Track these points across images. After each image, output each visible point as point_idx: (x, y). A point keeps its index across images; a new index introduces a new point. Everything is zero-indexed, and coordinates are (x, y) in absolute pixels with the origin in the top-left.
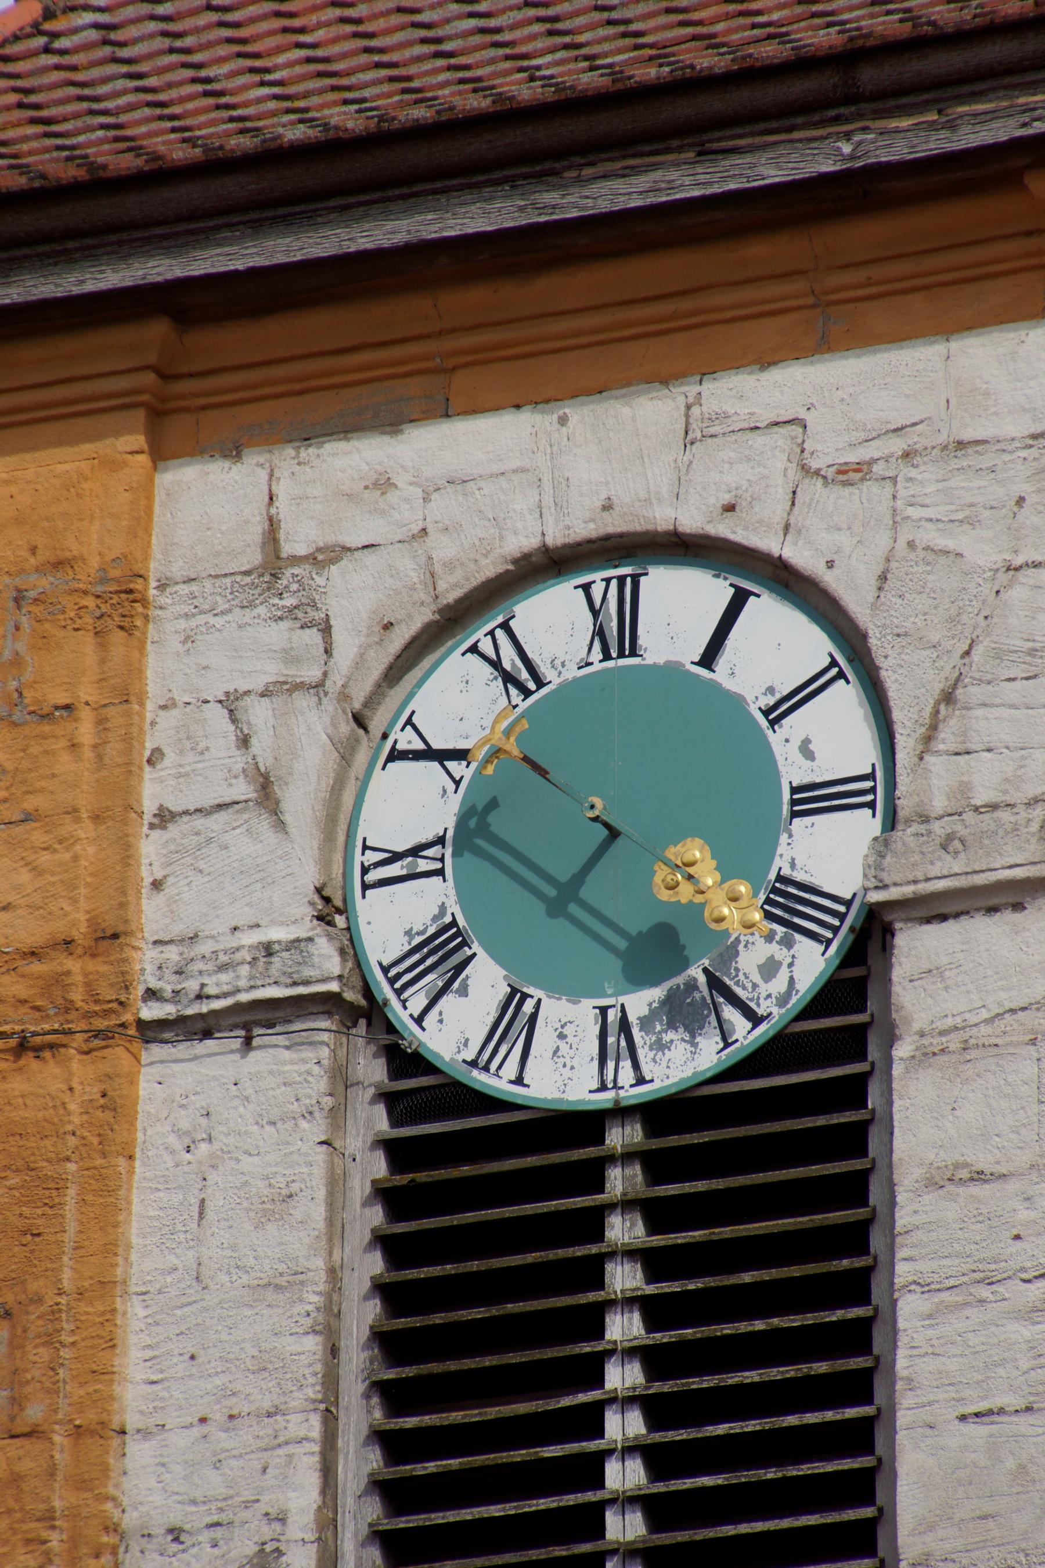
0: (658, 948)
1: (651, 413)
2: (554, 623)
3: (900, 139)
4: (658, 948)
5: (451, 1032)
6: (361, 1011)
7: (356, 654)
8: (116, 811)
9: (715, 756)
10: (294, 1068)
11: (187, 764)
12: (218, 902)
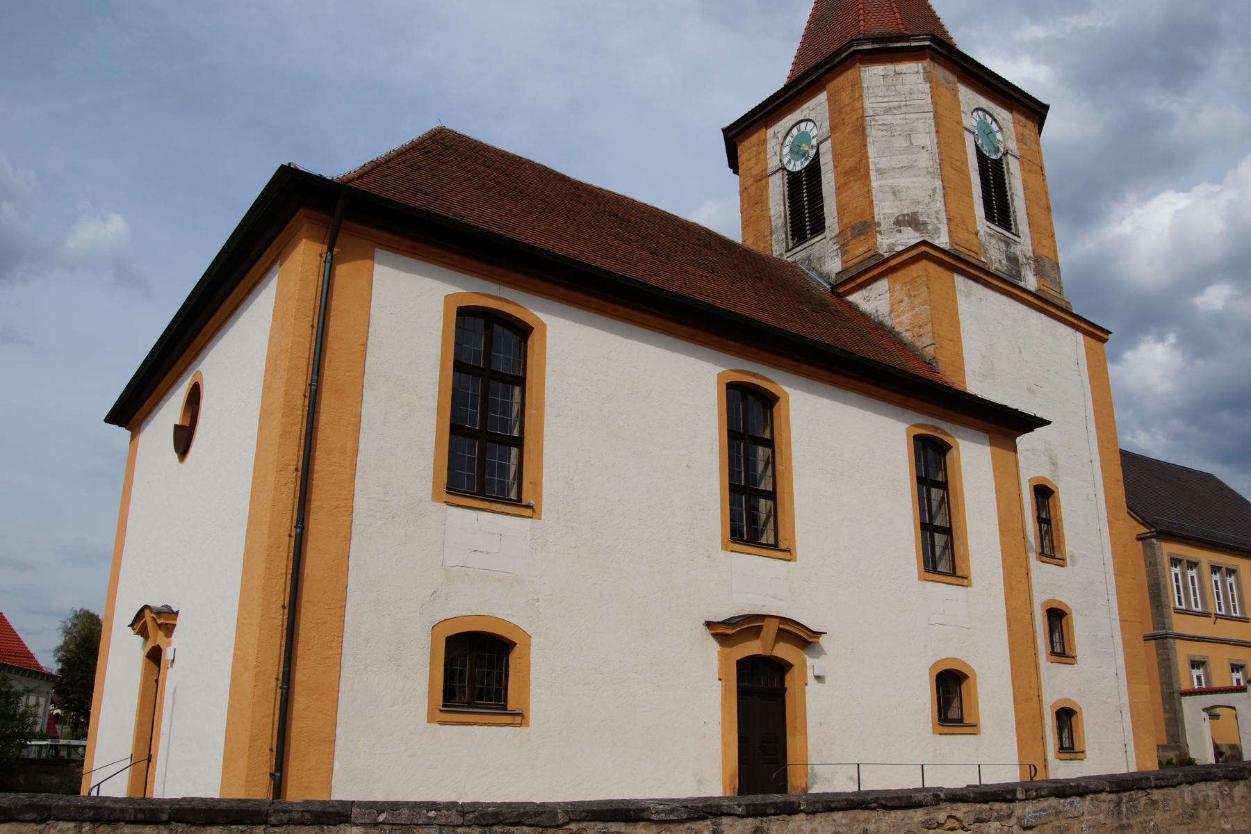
0: (804, 155)
1: (799, 111)
2: (795, 131)
3: (809, 80)
4: (804, 155)
5: (790, 168)
6: (784, 169)
7: (781, 140)
8: (766, 159)
9: (805, 136)
10: (779, 175)
11: (770, 153)
12: (773, 163)
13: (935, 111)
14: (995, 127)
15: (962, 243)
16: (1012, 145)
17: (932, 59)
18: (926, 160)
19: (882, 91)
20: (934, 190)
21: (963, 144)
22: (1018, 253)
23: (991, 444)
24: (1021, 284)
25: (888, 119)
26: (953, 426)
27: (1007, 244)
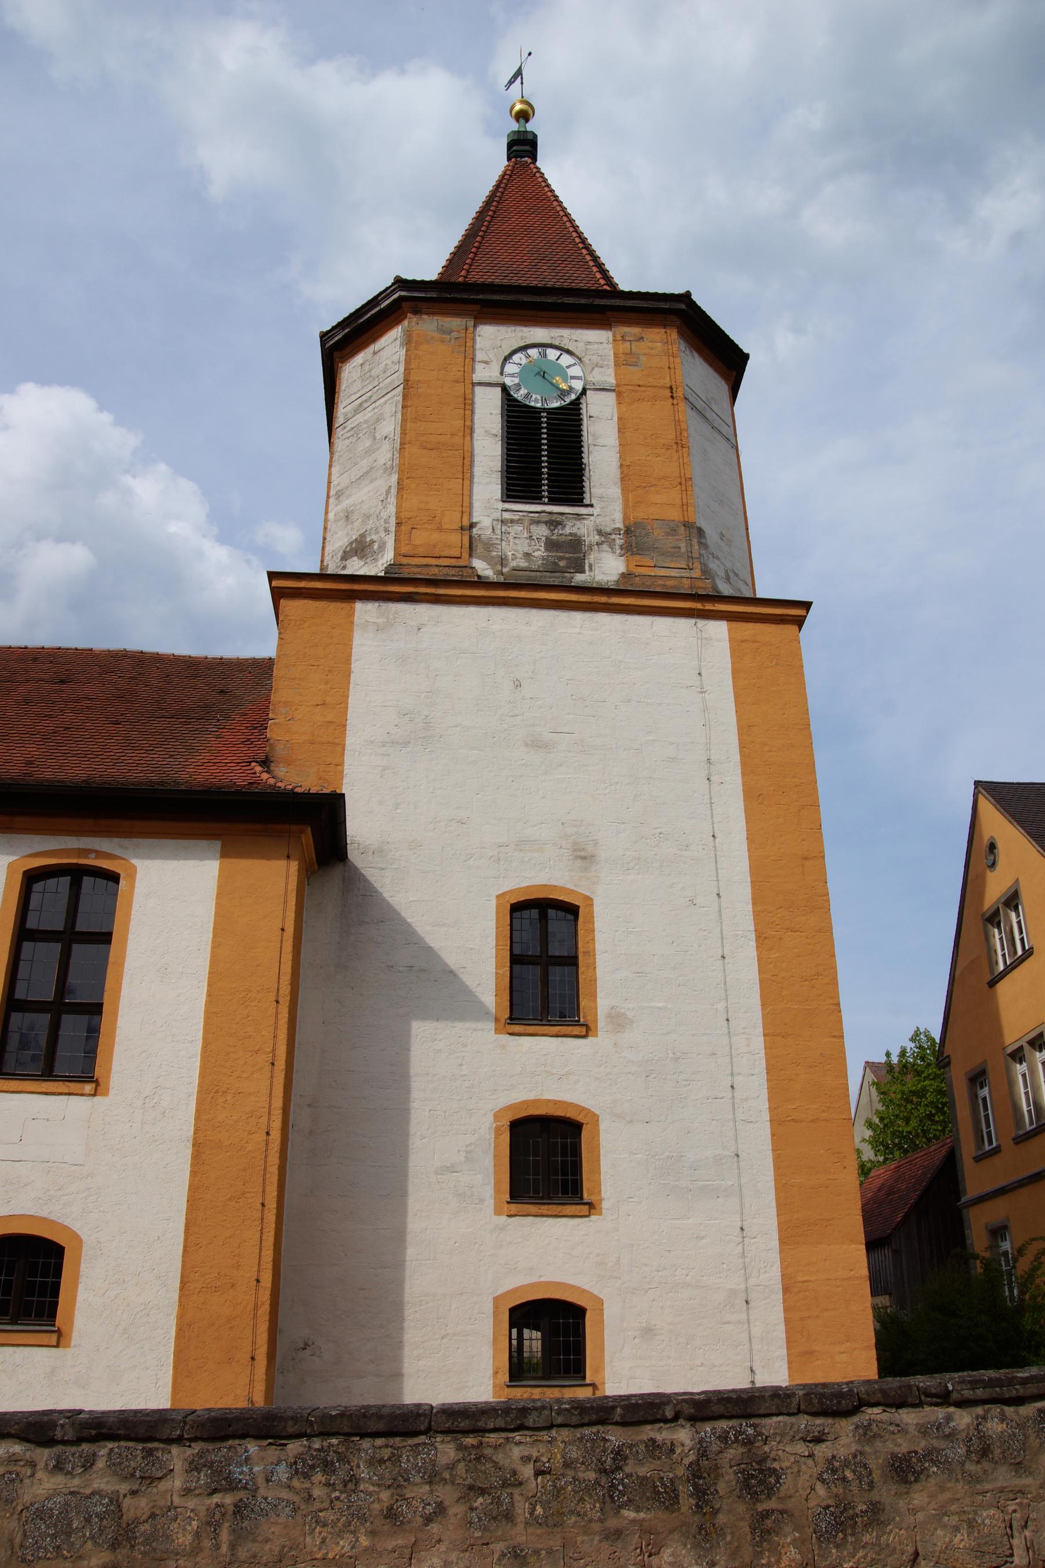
13: (406, 381)
14: (566, 360)
15: (421, 551)
16: (607, 376)
17: (416, 312)
18: (385, 454)
19: (358, 385)
20: (388, 492)
21: (468, 404)
22: (583, 531)
23: (224, 855)
24: (579, 578)
25: (359, 418)
26: (126, 842)
27: (554, 523)
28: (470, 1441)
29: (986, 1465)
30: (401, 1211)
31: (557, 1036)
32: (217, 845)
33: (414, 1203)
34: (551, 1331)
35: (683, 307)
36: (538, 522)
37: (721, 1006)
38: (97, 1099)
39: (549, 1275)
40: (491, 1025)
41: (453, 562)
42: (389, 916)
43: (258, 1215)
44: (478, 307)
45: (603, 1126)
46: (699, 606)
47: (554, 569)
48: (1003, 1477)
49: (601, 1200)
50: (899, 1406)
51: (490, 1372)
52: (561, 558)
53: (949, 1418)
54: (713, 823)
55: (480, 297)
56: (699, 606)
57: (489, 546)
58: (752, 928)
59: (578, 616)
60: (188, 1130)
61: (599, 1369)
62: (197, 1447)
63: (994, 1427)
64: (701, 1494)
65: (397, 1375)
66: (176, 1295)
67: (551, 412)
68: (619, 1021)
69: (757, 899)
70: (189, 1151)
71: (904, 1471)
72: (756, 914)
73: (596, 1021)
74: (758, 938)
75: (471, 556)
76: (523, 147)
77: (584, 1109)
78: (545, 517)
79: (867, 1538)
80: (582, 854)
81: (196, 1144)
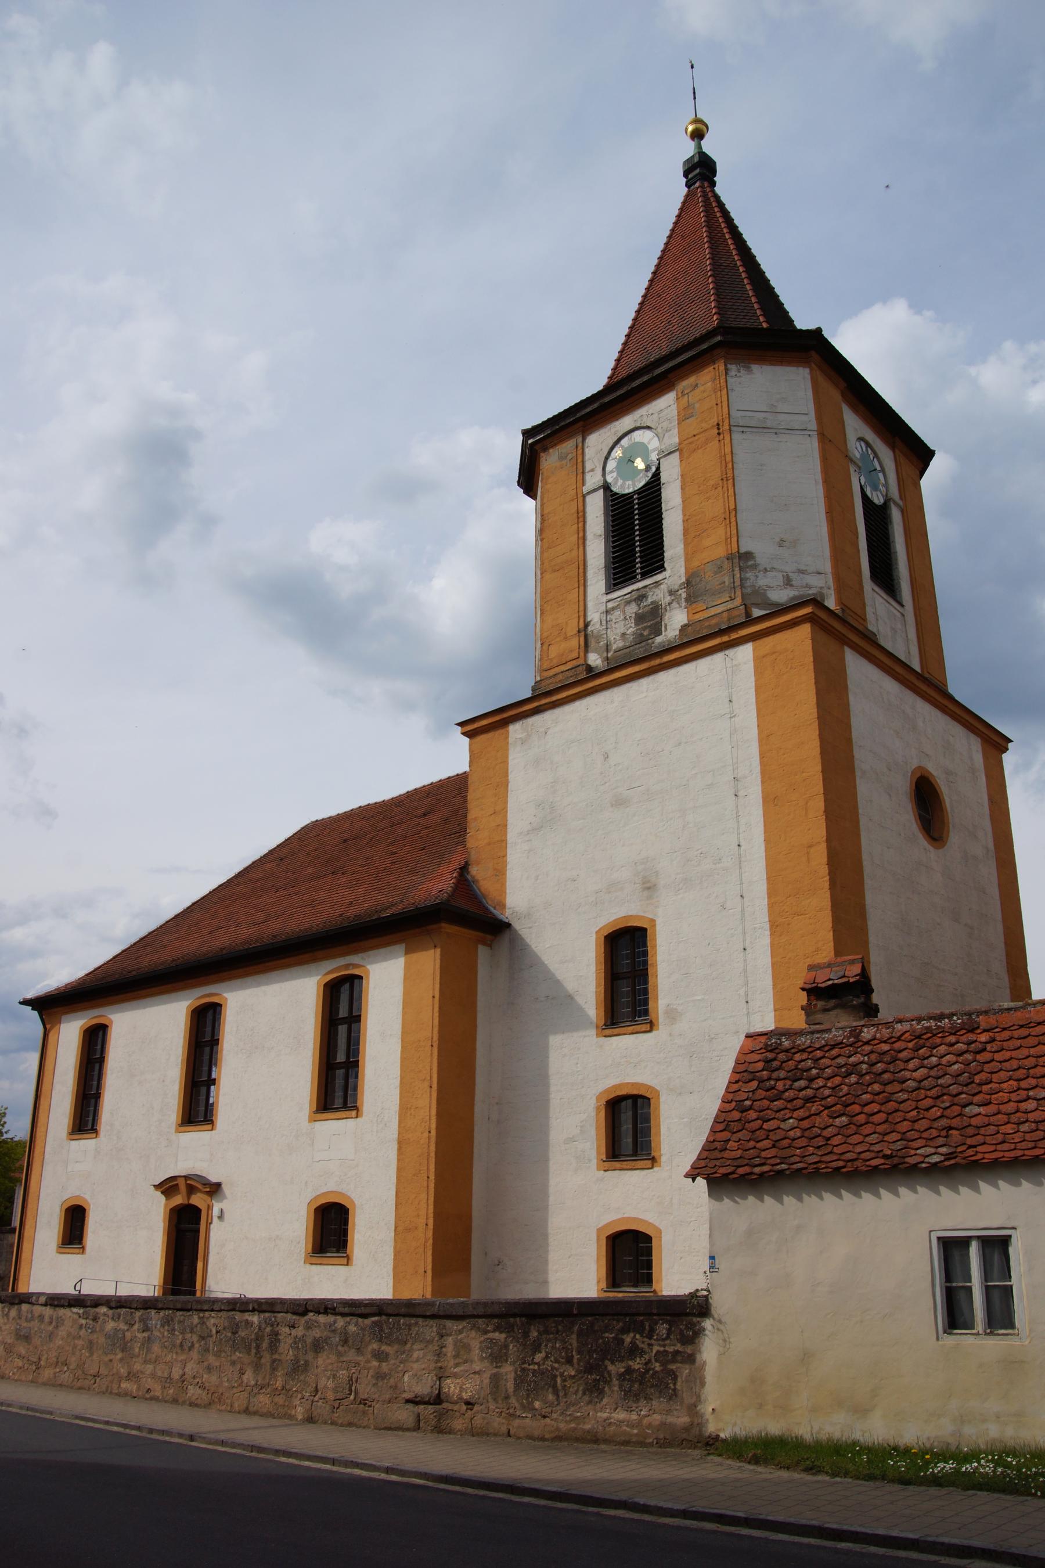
15: (555, 662)
17: (545, 449)
23: (408, 952)
28: (201, 1315)
29: (346, 1348)
30: (545, 1172)
31: (632, 1033)
32: (401, 948)
33: (553, 1166)
34: (630, 1251)
35: (719, 338)
36: (628, 603)
37: (742, 992)
38: (358, 1119)
39: (629, 1212)
40: (593, 1032)
41: (575, 663)
42: (536, 962)
43: (425, 1184)
44: (581, 424)
45: (662, 1099)
46: (725, 639)
47: (640, 639)
48: (351, 1355)
49: (660, 1156)
50: (319, 1313)
51: (595, 1282)
52: (644, 629)
53: (335, 1322)
54: (739, 834)
55: (578, 415)
56: (725, 639)
57: (598, 638)
58: (767, 919)
59: (644, 682)
60: (395, 1135)
61: (660, 1281)
62: (142, 1311)
63: (352, 1328)
64: (258, 1347)
65: (546, 1282)
66: (393, 1234)
67: (639, 492)
68: (673, 1015)
69: (771, 893)
70: (396, 1147)
71: (317, 1346)
72: (771, 906)
73: (657, 1018)
74: (771, 927)
75: (586, 651)
76: (701, 171)
77: (650, 1087)
78: (635, 595)
79: (302, 1378)
80: (648, 885)
81: (400, 1143)
